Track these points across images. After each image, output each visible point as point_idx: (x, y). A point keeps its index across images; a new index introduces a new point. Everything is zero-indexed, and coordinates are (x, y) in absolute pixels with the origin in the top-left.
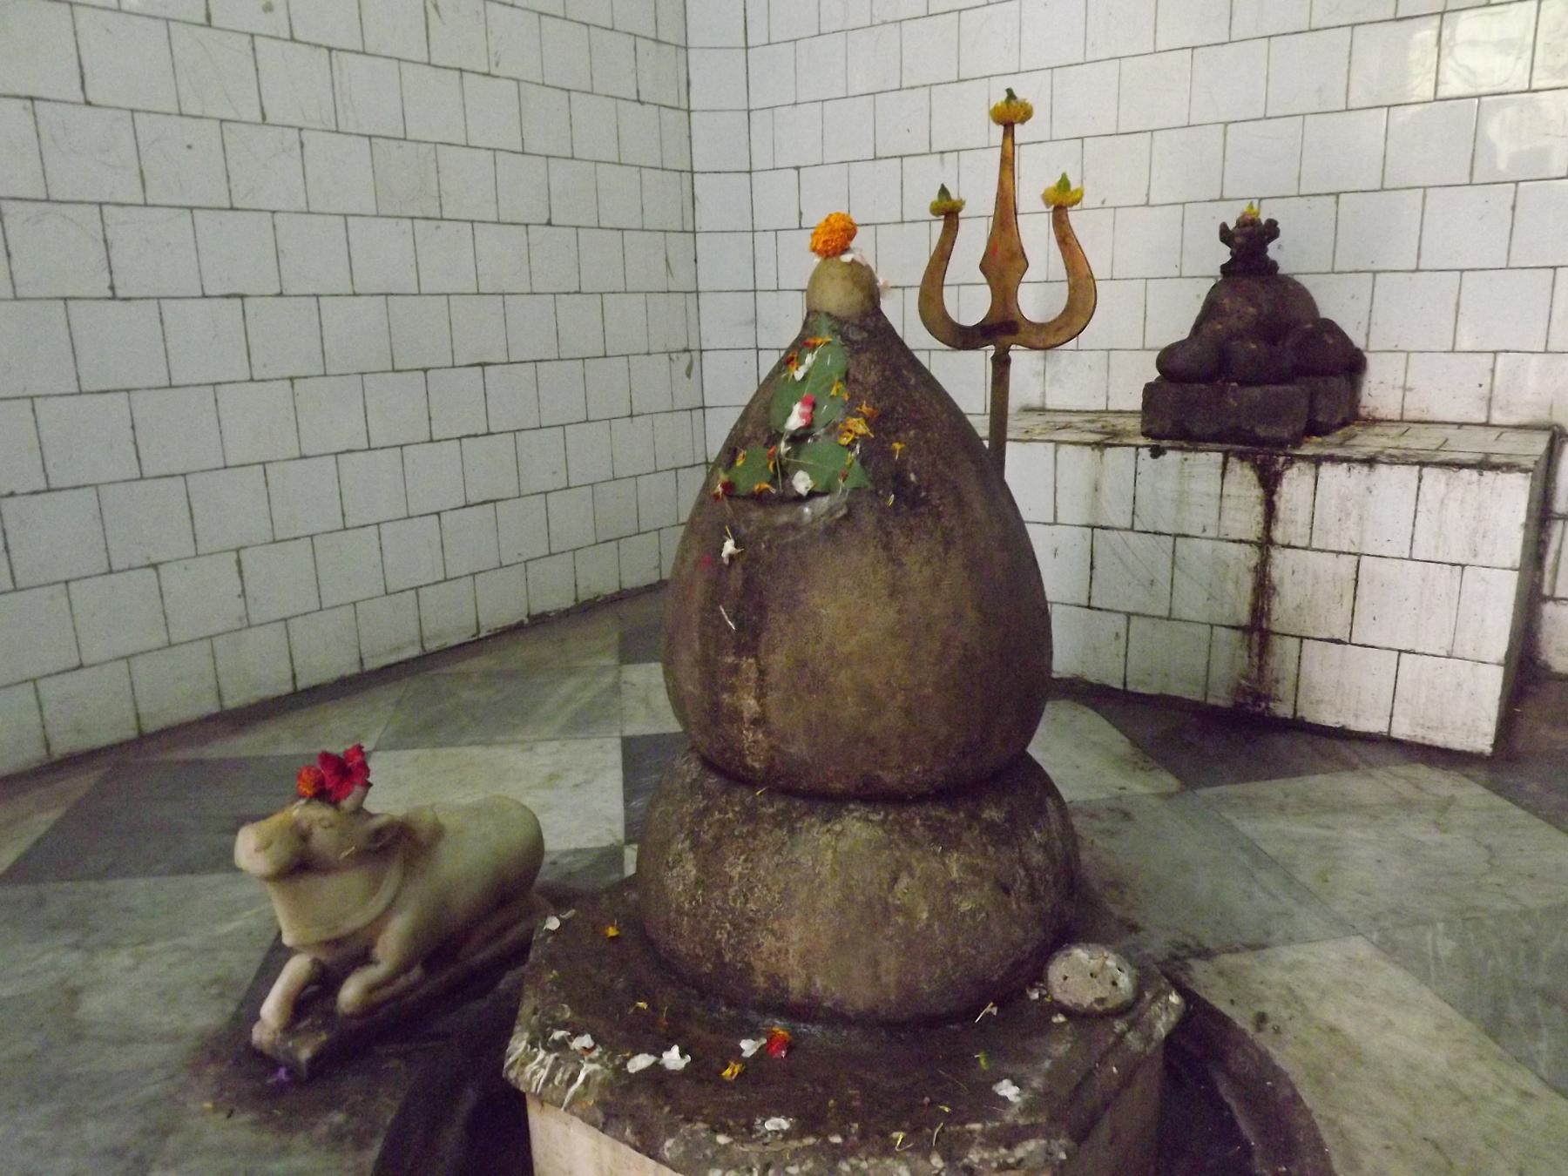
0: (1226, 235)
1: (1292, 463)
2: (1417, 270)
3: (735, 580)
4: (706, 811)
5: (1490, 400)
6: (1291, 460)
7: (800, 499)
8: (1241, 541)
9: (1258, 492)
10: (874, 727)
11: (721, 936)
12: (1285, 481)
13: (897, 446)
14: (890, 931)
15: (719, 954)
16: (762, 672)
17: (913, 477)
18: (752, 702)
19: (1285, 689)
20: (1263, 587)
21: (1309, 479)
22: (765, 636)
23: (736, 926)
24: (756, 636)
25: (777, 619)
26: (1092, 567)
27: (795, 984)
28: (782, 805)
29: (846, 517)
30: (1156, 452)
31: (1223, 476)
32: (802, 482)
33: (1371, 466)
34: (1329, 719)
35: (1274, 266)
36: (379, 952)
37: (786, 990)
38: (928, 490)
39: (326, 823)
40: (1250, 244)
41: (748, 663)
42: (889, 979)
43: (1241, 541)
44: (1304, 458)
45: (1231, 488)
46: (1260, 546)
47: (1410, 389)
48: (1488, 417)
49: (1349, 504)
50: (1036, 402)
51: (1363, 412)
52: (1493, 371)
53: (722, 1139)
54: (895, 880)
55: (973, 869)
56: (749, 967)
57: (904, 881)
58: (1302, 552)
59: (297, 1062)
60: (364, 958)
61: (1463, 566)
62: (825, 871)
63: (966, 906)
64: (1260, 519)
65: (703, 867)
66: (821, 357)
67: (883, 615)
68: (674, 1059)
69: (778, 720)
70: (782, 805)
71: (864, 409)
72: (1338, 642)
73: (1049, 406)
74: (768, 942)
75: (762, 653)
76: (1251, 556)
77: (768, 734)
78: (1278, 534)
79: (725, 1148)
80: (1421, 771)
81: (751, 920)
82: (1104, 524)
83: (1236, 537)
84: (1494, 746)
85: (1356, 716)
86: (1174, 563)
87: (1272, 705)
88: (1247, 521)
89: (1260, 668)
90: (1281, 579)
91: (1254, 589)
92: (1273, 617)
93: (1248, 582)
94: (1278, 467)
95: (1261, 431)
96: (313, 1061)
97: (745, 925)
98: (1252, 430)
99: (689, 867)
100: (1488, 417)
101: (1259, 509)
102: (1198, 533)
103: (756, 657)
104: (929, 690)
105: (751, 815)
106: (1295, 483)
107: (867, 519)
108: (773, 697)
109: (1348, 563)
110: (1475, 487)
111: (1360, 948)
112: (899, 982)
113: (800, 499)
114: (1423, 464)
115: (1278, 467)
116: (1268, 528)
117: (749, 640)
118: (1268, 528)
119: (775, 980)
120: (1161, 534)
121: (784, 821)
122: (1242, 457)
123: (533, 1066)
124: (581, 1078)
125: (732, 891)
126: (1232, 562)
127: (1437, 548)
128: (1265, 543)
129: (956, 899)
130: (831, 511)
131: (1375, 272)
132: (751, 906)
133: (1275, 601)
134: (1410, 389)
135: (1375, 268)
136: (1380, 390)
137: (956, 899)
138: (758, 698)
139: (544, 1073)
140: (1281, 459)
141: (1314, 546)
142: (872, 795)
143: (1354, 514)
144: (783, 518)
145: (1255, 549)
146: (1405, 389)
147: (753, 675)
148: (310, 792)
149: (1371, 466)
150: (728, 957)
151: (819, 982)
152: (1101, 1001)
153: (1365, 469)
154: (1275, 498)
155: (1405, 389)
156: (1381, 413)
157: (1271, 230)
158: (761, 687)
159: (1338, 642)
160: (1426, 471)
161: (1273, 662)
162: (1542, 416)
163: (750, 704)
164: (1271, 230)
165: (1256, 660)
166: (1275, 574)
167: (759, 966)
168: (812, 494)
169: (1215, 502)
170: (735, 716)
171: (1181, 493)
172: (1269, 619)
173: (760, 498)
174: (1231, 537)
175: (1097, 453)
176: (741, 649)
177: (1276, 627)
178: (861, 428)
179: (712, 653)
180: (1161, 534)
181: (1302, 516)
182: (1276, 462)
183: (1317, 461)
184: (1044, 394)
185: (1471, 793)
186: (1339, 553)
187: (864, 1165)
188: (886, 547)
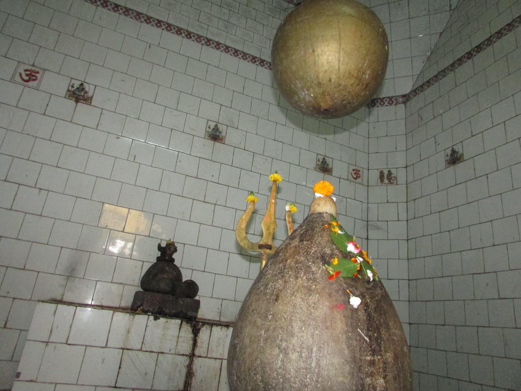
0: (160, 248)
2: (204, 271)
3: (362, 315)
8: (183, 355)
9: (191, 336)
12: (201, 332)
18: (382, 381)
20: (190, 374)
21: (209, 331)
26: (120, 368)
30: (156, 319)
31: (180, 328)
33: (228, 328)
35: (173, 260)
40: (167, 252)
43: (183, 355)
45: (182, 334)
46: (190, 357)
50: (59, 298)
52: (222, 305)
58: (204, 359)
64: (191, 346)
76: (185, 361)
78: (197, 353)
82: (129, 347)
83: (182, 354)
86: (156, 364)
88: (186, 347)
90: (196, 370)
91: (186, 374)
92: (193, 385)
93: (184, 371)
94: (199, 327)
98: (186, 313)
101: (191, 342)
102: (168, 351)
103: (381, 355)
106: (204, 333)
115: (199, 327)
116: (193, 350)
118: (193, 350)
120: (153, 352)
126: (179, 364)
128: (192, 356)
133: (194, 379)
138: (384, 378)
143: (222, 346)
145: (188, 357)
149: (228, 328)
154: (197, 338)
166: (194, 367)
169: (176, 339)
171: (163, 335)
172: (190, 387)
174: (180, 353)
175: (132, 317)
179: (358, 356)
180: (153, 352)
181: (205, 345)
182: (199, 324)
186: (216, 359)
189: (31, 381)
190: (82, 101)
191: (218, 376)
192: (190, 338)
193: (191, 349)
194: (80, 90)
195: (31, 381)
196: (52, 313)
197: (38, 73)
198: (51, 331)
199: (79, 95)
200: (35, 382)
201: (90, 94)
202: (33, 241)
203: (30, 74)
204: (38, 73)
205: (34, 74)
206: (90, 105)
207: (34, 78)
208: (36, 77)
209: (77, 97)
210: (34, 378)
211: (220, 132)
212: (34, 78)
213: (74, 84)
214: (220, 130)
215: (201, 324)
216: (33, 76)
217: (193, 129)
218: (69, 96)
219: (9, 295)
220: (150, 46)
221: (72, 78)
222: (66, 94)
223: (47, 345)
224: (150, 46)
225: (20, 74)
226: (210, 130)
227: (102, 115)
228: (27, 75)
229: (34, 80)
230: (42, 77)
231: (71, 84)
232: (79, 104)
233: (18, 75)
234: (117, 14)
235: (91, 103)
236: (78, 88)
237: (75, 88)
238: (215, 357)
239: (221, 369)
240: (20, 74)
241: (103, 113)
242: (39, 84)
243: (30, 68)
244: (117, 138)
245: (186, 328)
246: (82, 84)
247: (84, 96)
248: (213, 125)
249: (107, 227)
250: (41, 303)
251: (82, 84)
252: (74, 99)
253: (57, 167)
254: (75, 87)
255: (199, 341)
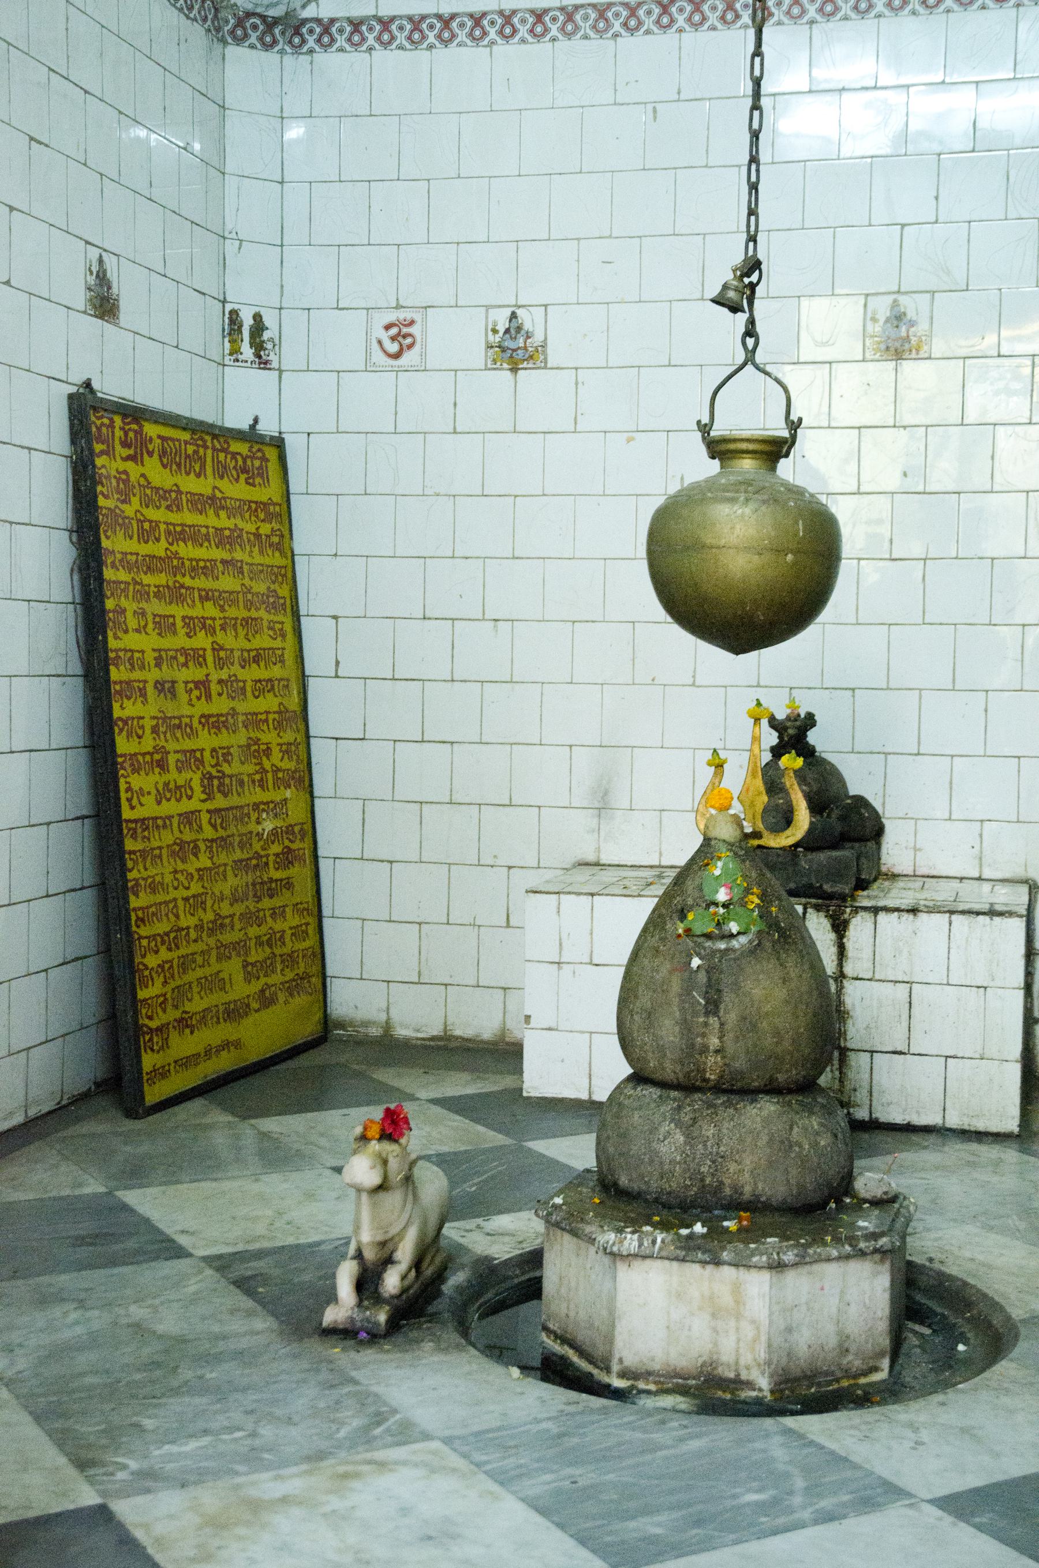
1: (857, 913)
2: (919, 754)
3: (702, 977)
4: (679, 1108)
5: (981, 858)
6: (856, 910)
7: (732, 936)
9: (833, 936)
10: (779, 1050)
11: (704, 1169)
12: (851, 927)
13: (773, 909)
14: (793, 1155)
15: (702, 1180)
16: (722, 1024)
17: (782, 925)
18: (717, 1041)
19: (861, 1096)
22: (722, 1006)
23: (714, 1162)
24: (717, 1007)
25: (728, 997)
27: (747, 1189)
28: (725, 1099)
29: (759, 945)
32: (734, 927)
33: (915, 915)
34: (897, 1117)
36: (398, 1255)
37: (741, 1194)
38: (790, 930)
39: (395, 1154)
41: (713, 1020)
42: (793, 1182)
44: (865, 909)
47: (920, 850)
48: (981, 872)
49: (901, 944)
50: (591, 858)
51: (884, 869)
52: (981, 836)
53: (752, 1246)
54: (791, 1129)
55: (821, 1124)
56: (722, 1183)
57: (796, 1130)
58: (868, 982)
59: (377, 1324)
60: (388, 1261)
61: (985, 988)
62: (759, 1126)
63: (823, 1143)
65: (688, 1136)
66: (725, 864)
67: (780, 993)
68: (699, 1228)
69: (730, 1049)
70: (725, 1099)
71: (755, 890)
72: (901, 1053)
73: (602, 862)
74: (733, 1167)
75: (721, 1014)
77: (723, 1057)
78: (849, 969)
79: (756, 1249)
80: (974, 1146)
81: (722, 1157)
84: (1020, 1126)
85: (918, 1112)
87: (851, 1110)
89: (841, 1081)
90: (853, 1005)
94: (846, 916)
95: (827, 887)
96: (388, 1321)
97: (718, 1160)
99: (677, 1136)
100: (981, 872)
104: (802, 1030)
105: (710, 1105)
106: (859, 928)
107: (768, 945)
108: (729, 1037)
109: (902, 990)
110: (988, 928)
111: (970, 1228)
112: (798, 1184)
113: (732, 936)
114: (952, 912)
115: (846, 916)
117: (713, 1006)
119: (737, 1189)
121: (728, 1104)
122: (818, 908)
123: (626, 1243)
124: (659, 1240)
125: (709, 1144)
127: (966, 975)
129: (819, 1139)
130: (750, 942)
131: (886, 754)
132: (722, 1148)
133: (850, 1022)
134: (920, 850)
135: (886, 751)
136: (896, 851)
137: (819, 1139)
139: (636, 1243)
140: (848, 910)
141: (877, 977)
142: (772, 1089)
144: (722, 945)
146: (916, 849)
147: (717, 1025)
148: (377, 1136)
149: (915, 915)
150: (708, 1181)
151: (760, 1186)
152: (885, 1193)
153: (911, 916)
154: (845, 940)
155: (916, 849)
156: (896, 870)
157: (810, 721)
158: (721, 1032)
159: (901, 1053)
160: (954, 917)
161: (851, 1074)
162: (1019, 872)
163: (714, 1042)
164: (810, 721)
165: (837, 1073)
167: (727, 1182)
168: (739, 933)
170: (704, 1050)
173: (708, 936)
176: (707, 1014)
177: (850, 1045)
178: (757, 901)
179: (689, 1017)
181: (867, 953)
182: (844, 912)
183: (876, 910)
184: (598, 850)
185: (1011, 1155)
186: (896, 982)
187: (818, 1250)
188: (778, 959)
189: (550, 1029)
190: (525, 365)
191: (905, 1016)
192: (828, 942)
193: (835, 963)
194: (513, 331)
195: (550, 1029)
196: (555, 910)
197: (412, 323)
198: (561, 944)
199: (514, 349)
200: (557, 1030)
201: (538, 338)
202: (512, 741)
203: (399, 334)
204: (412, 323)
205: (405, 330)
206: (545, 368)
207: (409, 340)
208: (410, 335)
209: (511, 357)
210: (553, 1025)
211: (912, 324)
212: (409, 340)
213: (495, 324)
214: (911, 314)
215: (848, 910)
216: (405, 337)
217: (824, 344)
218: (495, 361)
219: (499, 862)
220: (655, 110)
221: (488, 307)
222: (486, 356)
223: (559, 969)
224: (655, 110)
225: (380, 342)
226: (878, 328)
227: (580, 385)
228: (393, 339)
229: (410, 347)
230: (425, 332)
231: (490, 327)
232: (520, 372)
233: (375, 346)
234: (545, 47)
235: (546, 363)
236: (507, 331)
237: (501, 334)
238: (893, 979)
239: (910, 1003)
240: (380, 342)
241: (580, 380)
242: (423, 355)
243: (391, 317)
244: (629, 440)
245: (816, 920)
246: (514, 315)
247: (525, 348)
248: (882, 307)
249: (655, 682)
250: (531, 895)
251: (514, 315)
252: (505, 366)
253: (514, 558)
254: (502, 330)
255: (850, 944)
